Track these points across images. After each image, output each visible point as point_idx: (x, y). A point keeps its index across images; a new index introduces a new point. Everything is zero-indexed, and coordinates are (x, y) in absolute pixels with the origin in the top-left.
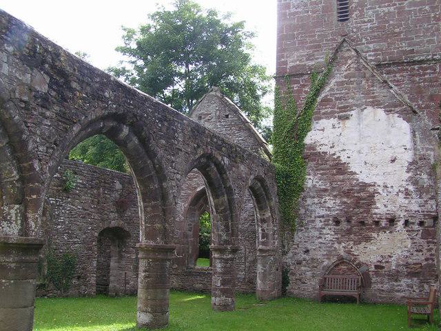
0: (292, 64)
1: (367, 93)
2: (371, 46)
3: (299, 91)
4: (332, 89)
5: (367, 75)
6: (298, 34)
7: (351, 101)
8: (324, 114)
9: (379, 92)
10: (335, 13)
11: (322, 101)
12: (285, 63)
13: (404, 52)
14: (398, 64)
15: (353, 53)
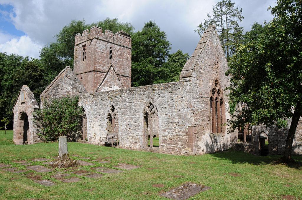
0: (98, 68)
1: (115, 81)
2: (117, 69)
3: (100, 77)
4: (107, 78)
5: (115, 77)
6: (100, 58)
7: (112, 83)
8: (106, 85)
9: (117, 81)
10: (109, 56)
11: (105, 81)
12: (96, 67)
13: (123, 73)
14: (122, 75)
15: (113, 69)
